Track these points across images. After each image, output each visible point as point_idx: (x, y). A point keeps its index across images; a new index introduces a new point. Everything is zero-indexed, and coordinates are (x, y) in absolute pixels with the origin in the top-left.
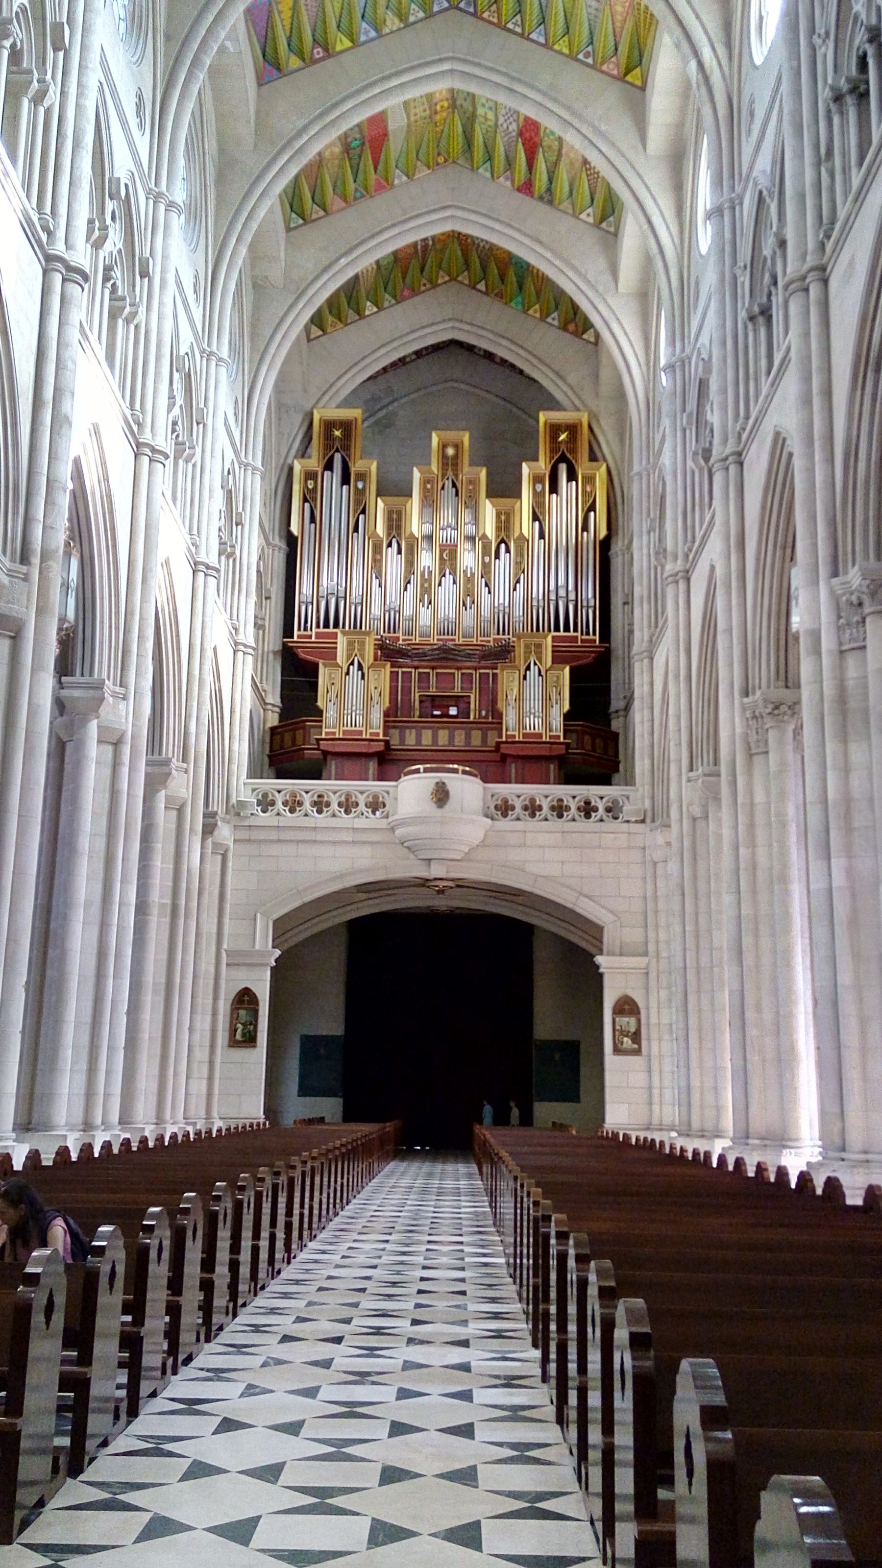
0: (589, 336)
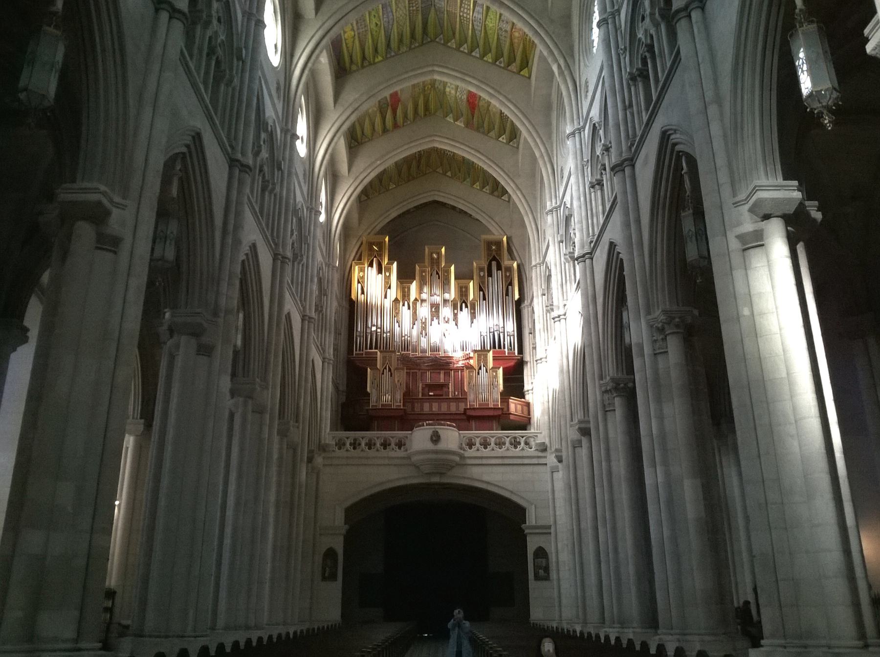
0: (505, 198)
